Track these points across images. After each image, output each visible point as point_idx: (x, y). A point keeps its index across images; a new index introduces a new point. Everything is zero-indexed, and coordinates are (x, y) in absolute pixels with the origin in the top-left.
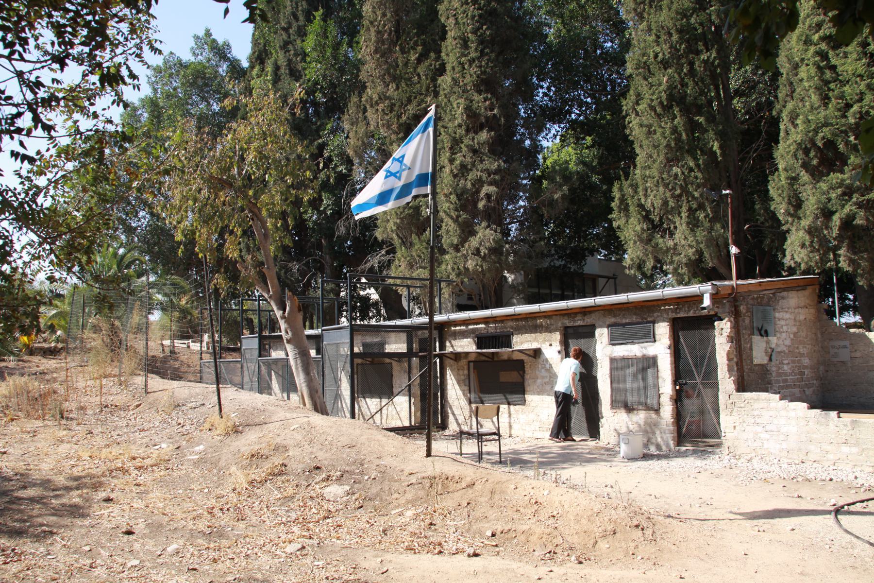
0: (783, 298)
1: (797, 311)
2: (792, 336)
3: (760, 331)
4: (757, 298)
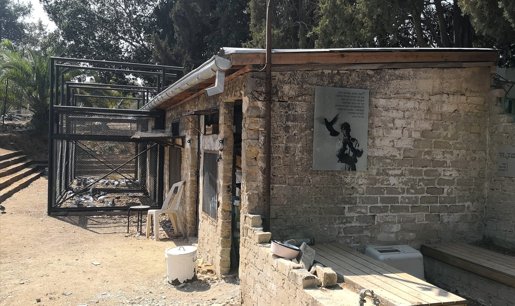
0: (402, 78)
1: (434, 98)
2: (416, 135)
3: (329, 125)
4: (331, 76)
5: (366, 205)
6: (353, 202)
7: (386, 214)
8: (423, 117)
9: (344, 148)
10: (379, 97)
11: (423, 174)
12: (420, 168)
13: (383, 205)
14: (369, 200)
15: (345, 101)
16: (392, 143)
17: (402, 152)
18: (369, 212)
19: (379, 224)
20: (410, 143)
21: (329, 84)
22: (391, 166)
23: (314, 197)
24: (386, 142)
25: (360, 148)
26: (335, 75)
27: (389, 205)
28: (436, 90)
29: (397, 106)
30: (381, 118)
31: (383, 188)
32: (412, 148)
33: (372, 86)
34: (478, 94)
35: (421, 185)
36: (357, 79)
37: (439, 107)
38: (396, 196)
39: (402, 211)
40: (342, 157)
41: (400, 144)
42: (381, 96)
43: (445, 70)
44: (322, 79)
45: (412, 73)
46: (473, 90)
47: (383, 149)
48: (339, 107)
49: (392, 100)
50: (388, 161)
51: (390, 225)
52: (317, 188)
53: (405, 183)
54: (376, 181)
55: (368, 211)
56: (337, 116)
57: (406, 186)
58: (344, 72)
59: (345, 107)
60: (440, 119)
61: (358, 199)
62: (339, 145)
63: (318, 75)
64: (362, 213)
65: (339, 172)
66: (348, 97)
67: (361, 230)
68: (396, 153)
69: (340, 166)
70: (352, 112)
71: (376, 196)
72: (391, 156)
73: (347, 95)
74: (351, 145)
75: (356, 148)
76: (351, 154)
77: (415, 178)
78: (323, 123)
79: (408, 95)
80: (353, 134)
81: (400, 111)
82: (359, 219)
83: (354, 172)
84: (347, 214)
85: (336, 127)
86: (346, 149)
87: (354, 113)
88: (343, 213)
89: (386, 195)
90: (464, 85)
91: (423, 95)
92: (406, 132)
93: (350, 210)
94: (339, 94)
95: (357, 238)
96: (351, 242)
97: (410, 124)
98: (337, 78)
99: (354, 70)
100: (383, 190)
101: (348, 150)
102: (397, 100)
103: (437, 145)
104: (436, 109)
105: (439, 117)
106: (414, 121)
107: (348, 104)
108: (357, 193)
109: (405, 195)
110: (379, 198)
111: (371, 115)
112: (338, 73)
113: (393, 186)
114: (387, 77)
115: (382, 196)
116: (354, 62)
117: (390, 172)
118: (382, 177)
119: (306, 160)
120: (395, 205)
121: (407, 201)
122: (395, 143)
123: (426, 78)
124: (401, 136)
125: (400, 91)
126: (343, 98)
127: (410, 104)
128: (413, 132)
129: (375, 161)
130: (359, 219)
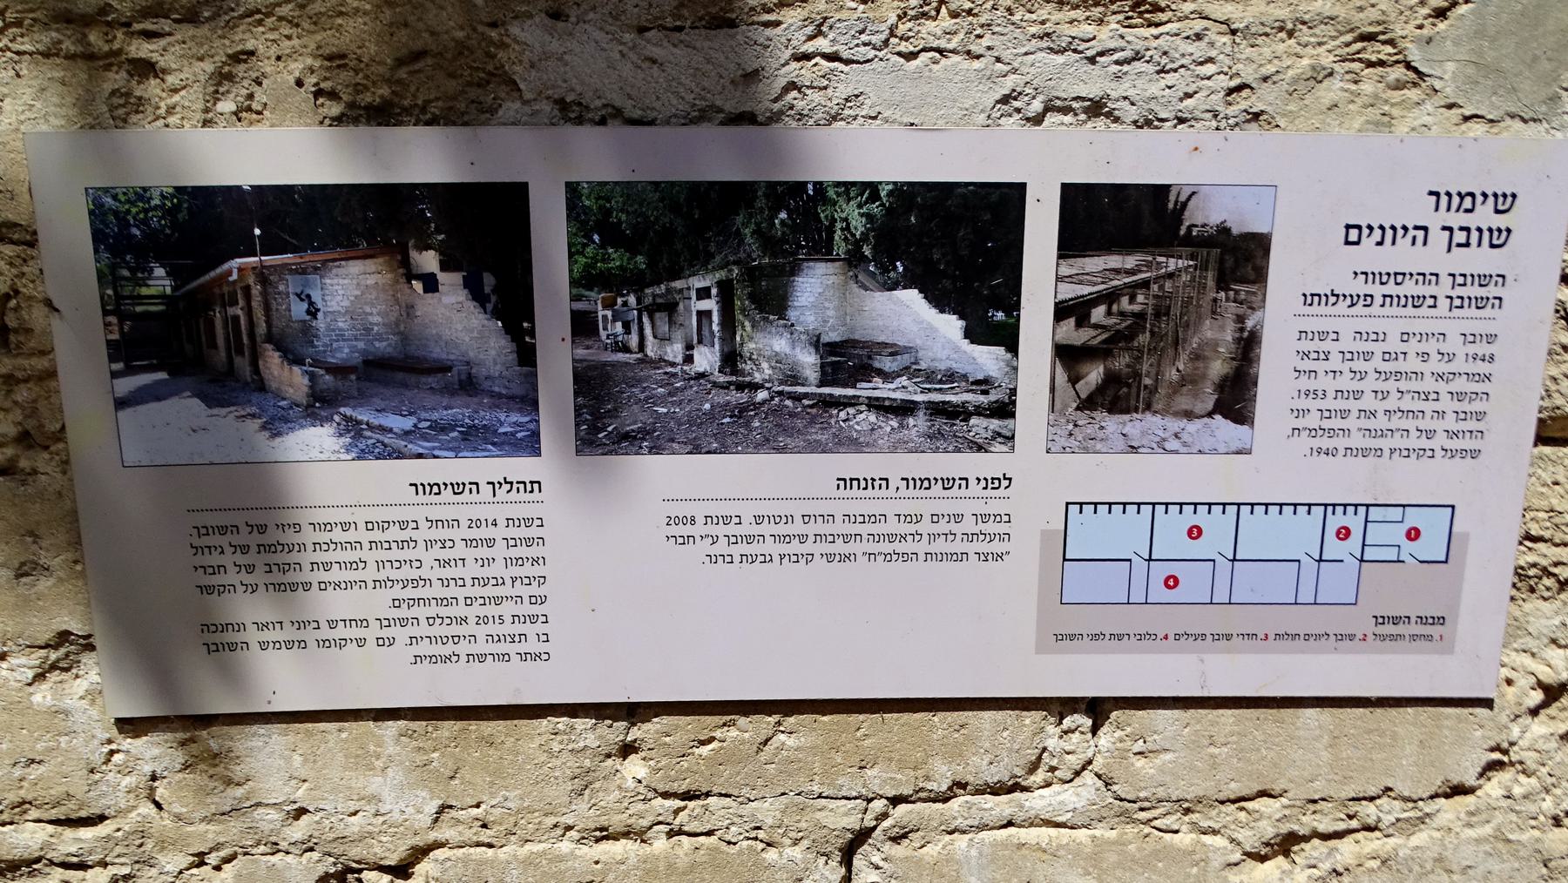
0: (339, 267)
2: (353, 298)
3: (298, 296)
14: (328, 336)
24: (333, 303)
41: (342, 304)
62: (305, 306)
68: (340, 309)
69: (308, 318)
85: (303, 297)
103: (366, 304)
104: (363, 282)
111: (322, 289)
127: (346, 281)
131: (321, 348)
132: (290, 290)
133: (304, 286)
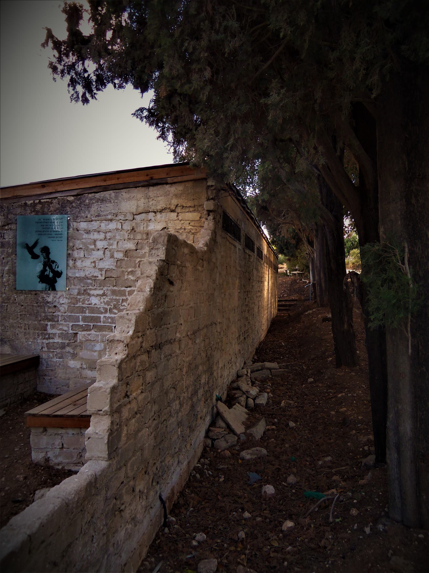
0: (103, 201)
1: (138, 217)
3: (30, 249)
5: (68, 323)
6: (56, 320)
7: (88, 333)
8: (126, 237)
9: (44, 270)
10: (79, 221)
11: (127, 294)
12: (126, 289)
13: (85, 324)
15: (45, 227)
16: (93, 265)
17: (103, 272)
18: (70, 330)
19: (81, 342)
20: (113, 264)
21: (31, 213)
22: (92, 286)
23: (19, 314)
24: (87, 263)
25: (59, 270)
26: (37, 204)
27: (92, 324)
28: (140, 210)
29: (98, 228)
30: (82, 240)
31: (84, 308)
32: (114, 268)
33: (72, 211)
34: (191, 209)
35: (124, 305)
36: (58, 206)
37: (145, 225)
38: (98, 315)
39: (105, 331)
40: (43, 278)
41: (101, 265)
42: (82, 219)
43: (151, 188)
44: (25, 209)
45: (113, 195)
46: (185, 205)
47: (84, 270)
48: (39, 233)
49: (93, 223)
50: (89, 281)
51: (93, 344)
52: (22, 306)
53: (108, 303)
54: (78, 301)
55: (70, 328)
56: (37, 240)
57: (108, 306)
58: (45, 200)
59: (44, 233)
60: (145, 238)
61: (60, 317)
62: (39, 267)
63: (21, 205)
64: (63, 330)
65: (42, 291)
66: (47, 222)
67: (63, 346)
68: (97, 273)
69: (41, 286)
70: (51, 236)
71: (77, 315)
72: (93, 276)
73: (46, 221)
74: (51, 267)
75: (56, 269)
76: (51, 275)
77: (118, 298)
78: (25, 248)
79: (110, 217)
80: (52, 257)
81: (101, 233)
82: (61, 336)
83: (55, 292)
84: (50, 330)
85: (37, 251)
86: (46, 270)
87: (53, 237)
88: (46, 330)
89: (87, 315)
90: (175, 202)
91: (125, 216)
92: (108, 253)
93: (53, 327)
94: (39, 221)
95: (59, 353)
96: (54, 357)
97: (112, 245)
98: (39, 207)
99: (56, 198)
100: (85, 310)
101: (48, 272)
102: (98, 222)
105: (145, 237)
106: (116, 242)
107: (47, 230)
108: (59, 311)
109: (108, 315)
110: (81, 317)
112: (40, 202)
113: (95, 306)
114: (87, 201)
115: (83, 315)
116: (54, 191)
117: (92, 292)
118: (83, 297)
119: (12, 281)
120: (98, 324)
121: (110, 320)
122: (97, 264)
123: (129, 199)
124: (102, 256)
125: (101, 213)
126: (42, 224)
127: (112, 226)
128: (115, 253)
129: (76, 281)
130: (61, 336)
131: (57, 340)
132: (19, 240)
133: (40, 233)
